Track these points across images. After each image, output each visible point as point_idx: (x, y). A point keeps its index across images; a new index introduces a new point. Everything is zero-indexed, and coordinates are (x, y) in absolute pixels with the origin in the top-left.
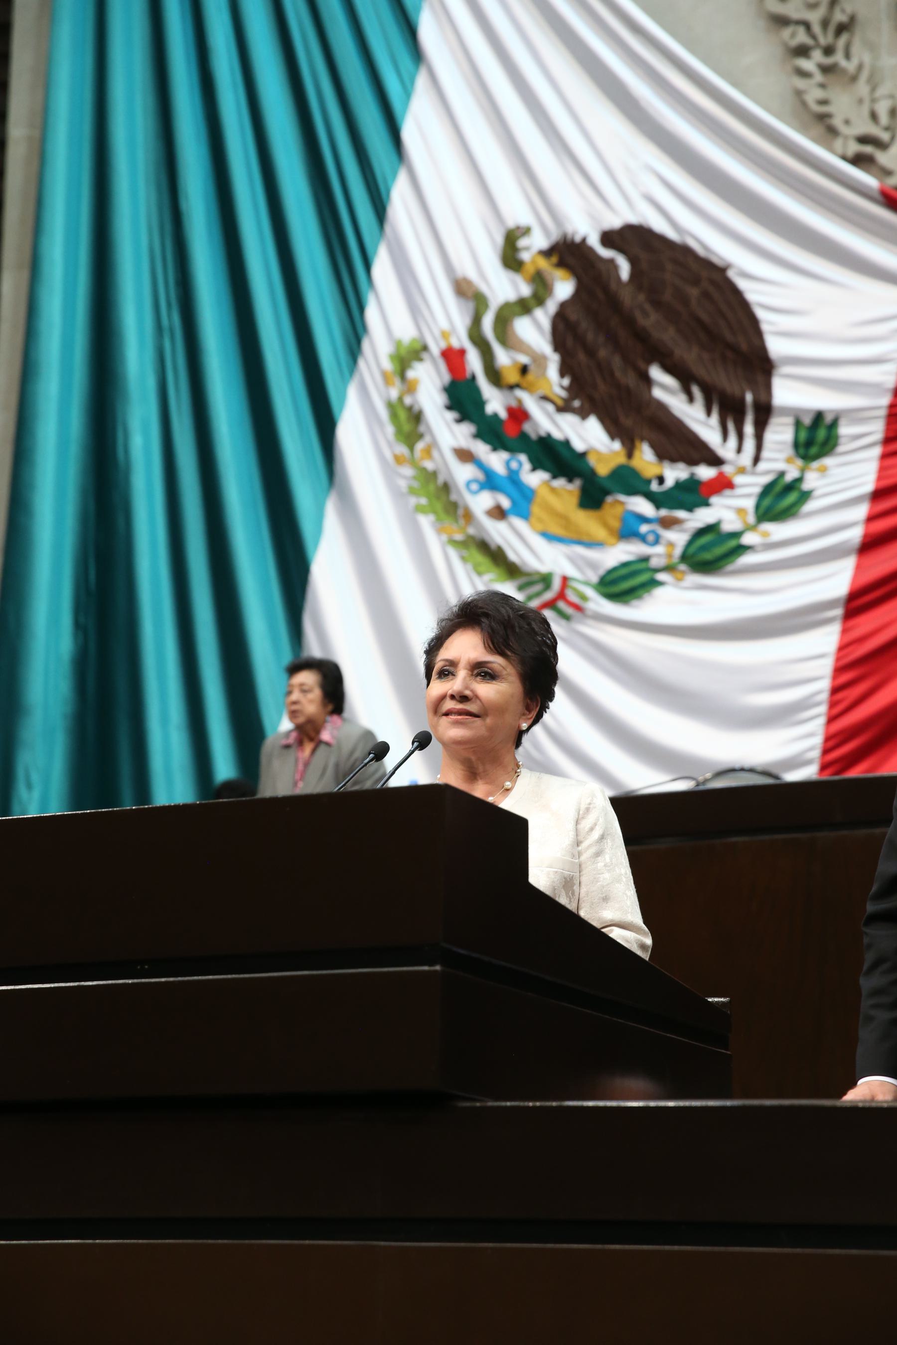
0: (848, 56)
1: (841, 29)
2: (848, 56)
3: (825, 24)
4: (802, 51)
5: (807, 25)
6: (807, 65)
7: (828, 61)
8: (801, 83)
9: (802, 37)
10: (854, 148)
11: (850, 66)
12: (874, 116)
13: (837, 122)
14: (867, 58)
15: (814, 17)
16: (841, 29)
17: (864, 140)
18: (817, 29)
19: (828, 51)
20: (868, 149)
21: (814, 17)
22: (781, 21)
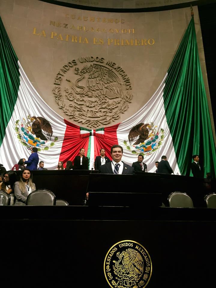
0: (61, 98)
1: (60, 96)
2: (61, 98)
3: (59, 95)
4: (56, 97)
5: (57, 95)
6: (57, 98)
7: (59, 99)
8: (56, 100)
9: (56, 96)
10: (61, 107)
11: (61, 100)
12: (63, 105)
13: (59, 105)
14: (63, 100)
15: (58, 94)
16: (60, 96)
17: (62, 107)
18: (58, 95)
19: (59, 98)
20: (62, 108)
21: (58, 94)
22: (55, 94)
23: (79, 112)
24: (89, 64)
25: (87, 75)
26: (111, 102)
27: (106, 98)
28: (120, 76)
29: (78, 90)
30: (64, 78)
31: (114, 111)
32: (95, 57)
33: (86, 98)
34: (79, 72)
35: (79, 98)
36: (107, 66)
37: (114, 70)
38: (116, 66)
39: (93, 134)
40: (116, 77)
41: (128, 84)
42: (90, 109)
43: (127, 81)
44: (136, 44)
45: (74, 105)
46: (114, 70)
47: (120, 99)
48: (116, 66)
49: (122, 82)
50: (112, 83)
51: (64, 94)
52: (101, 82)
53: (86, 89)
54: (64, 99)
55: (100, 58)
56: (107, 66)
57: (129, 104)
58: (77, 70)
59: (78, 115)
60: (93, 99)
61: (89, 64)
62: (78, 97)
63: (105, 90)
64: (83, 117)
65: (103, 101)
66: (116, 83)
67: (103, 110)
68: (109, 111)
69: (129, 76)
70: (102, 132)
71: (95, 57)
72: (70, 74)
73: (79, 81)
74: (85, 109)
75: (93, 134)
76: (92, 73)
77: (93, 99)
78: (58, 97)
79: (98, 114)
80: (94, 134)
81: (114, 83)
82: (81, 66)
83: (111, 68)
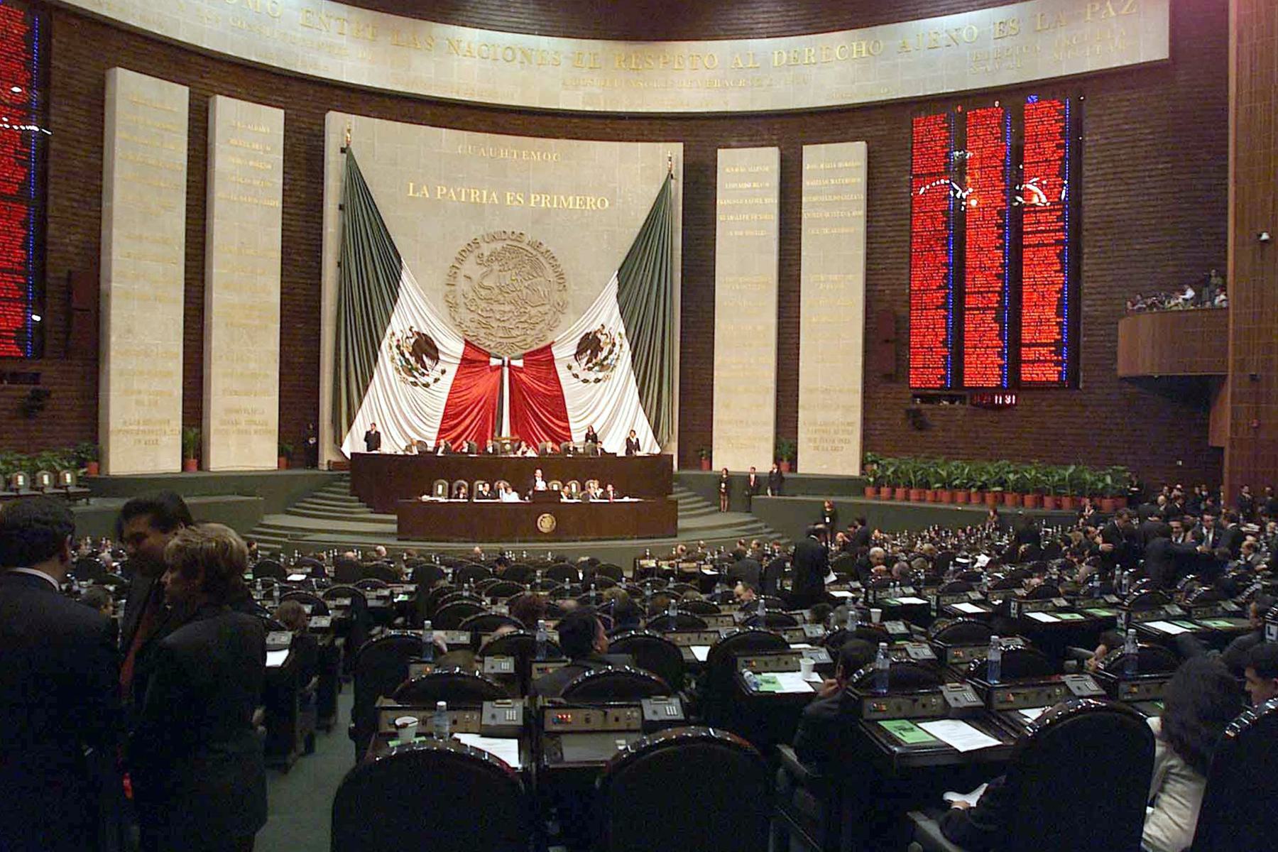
23: (484, 330)
24: (498, 246)
25: (496, 266)
26: (533, 312)
27: (526, 306)
28: (549, 270)
29: (483, 292)
30: (461, 274)
31: (538, 327)
32: (509, 231)
33: (496, 307)
34: (485, 259)
35: (486, 305)
36: (528, 248)
37: (539, 256)
38: (543, 249)
39: (506, 363)
40: (542, 268)
41: (561, 281)
42: (502, 324)
43: (560, 276)
44: (578, 207)
45: (477, 317)
46: (539, 256)
47: (548, 307)
48: (543, 249)
49: (552, 277)
50: (535, 280)
51: (461, 300)
52: (519, 278)
53: (497, 291)
54: (462, 310)
55: (518, 232)
56: (528, 248)
57: (560, 316)
58: (480, 256)
59: (483, 335)
60: (507, 308)
61: (498, 246)
62: (484, 305)
63: (525, 291)
64: (491, 337)
65: (522, 310)
66: (542, 279)
67: (520, 325)
68: (531, 326)
69: (565, 267)
70: (520, 363)
71: (509, 231)
72: (470, 267)
73: (484, 276)
74: (495, 324)
75: (506, 363)
76: (503, 262)
77: (507, 308)
78: (453, 306)
79: (514, 333)
80: (509, 366)
81: (539, 279)
82: (486, 249)
83: (534, 253)
